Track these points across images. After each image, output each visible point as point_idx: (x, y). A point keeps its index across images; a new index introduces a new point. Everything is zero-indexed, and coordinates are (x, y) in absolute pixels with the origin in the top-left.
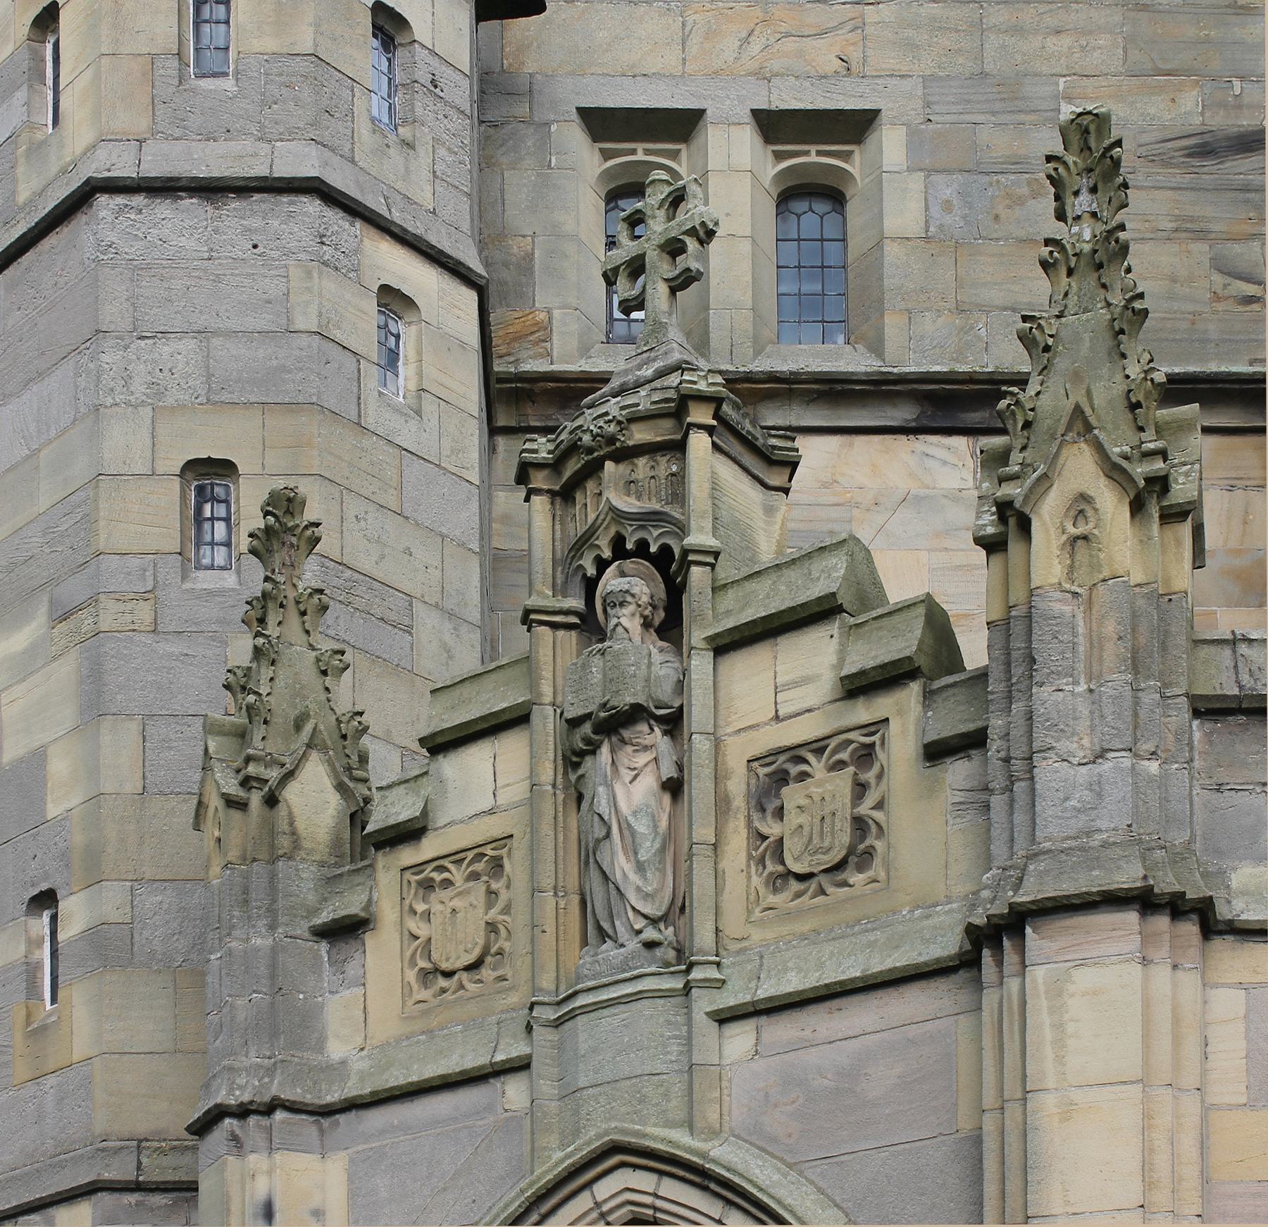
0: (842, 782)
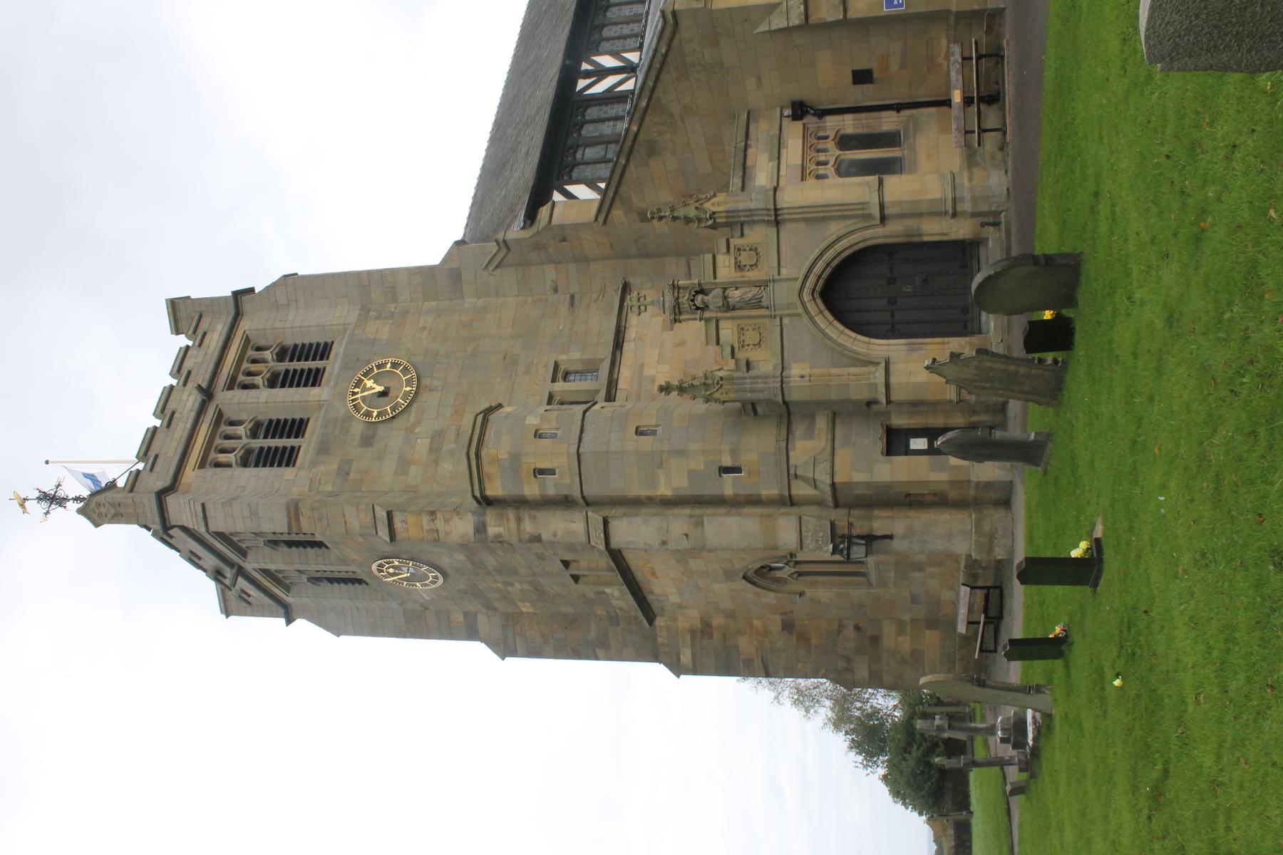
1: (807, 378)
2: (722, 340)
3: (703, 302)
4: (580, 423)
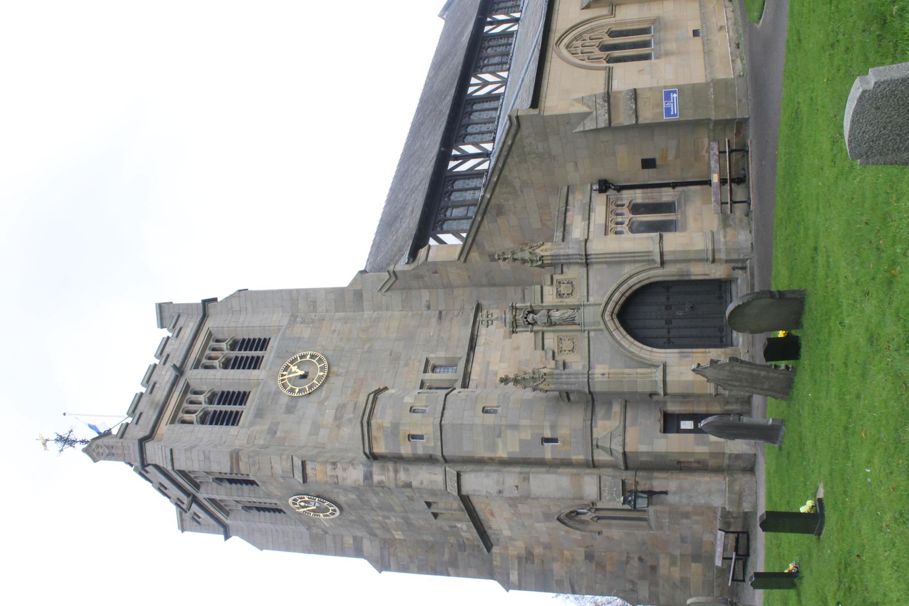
0: (562, 285)
1: (607, 376)
2: (546, 347)
3: (533, 319)
4: (443, 402)
